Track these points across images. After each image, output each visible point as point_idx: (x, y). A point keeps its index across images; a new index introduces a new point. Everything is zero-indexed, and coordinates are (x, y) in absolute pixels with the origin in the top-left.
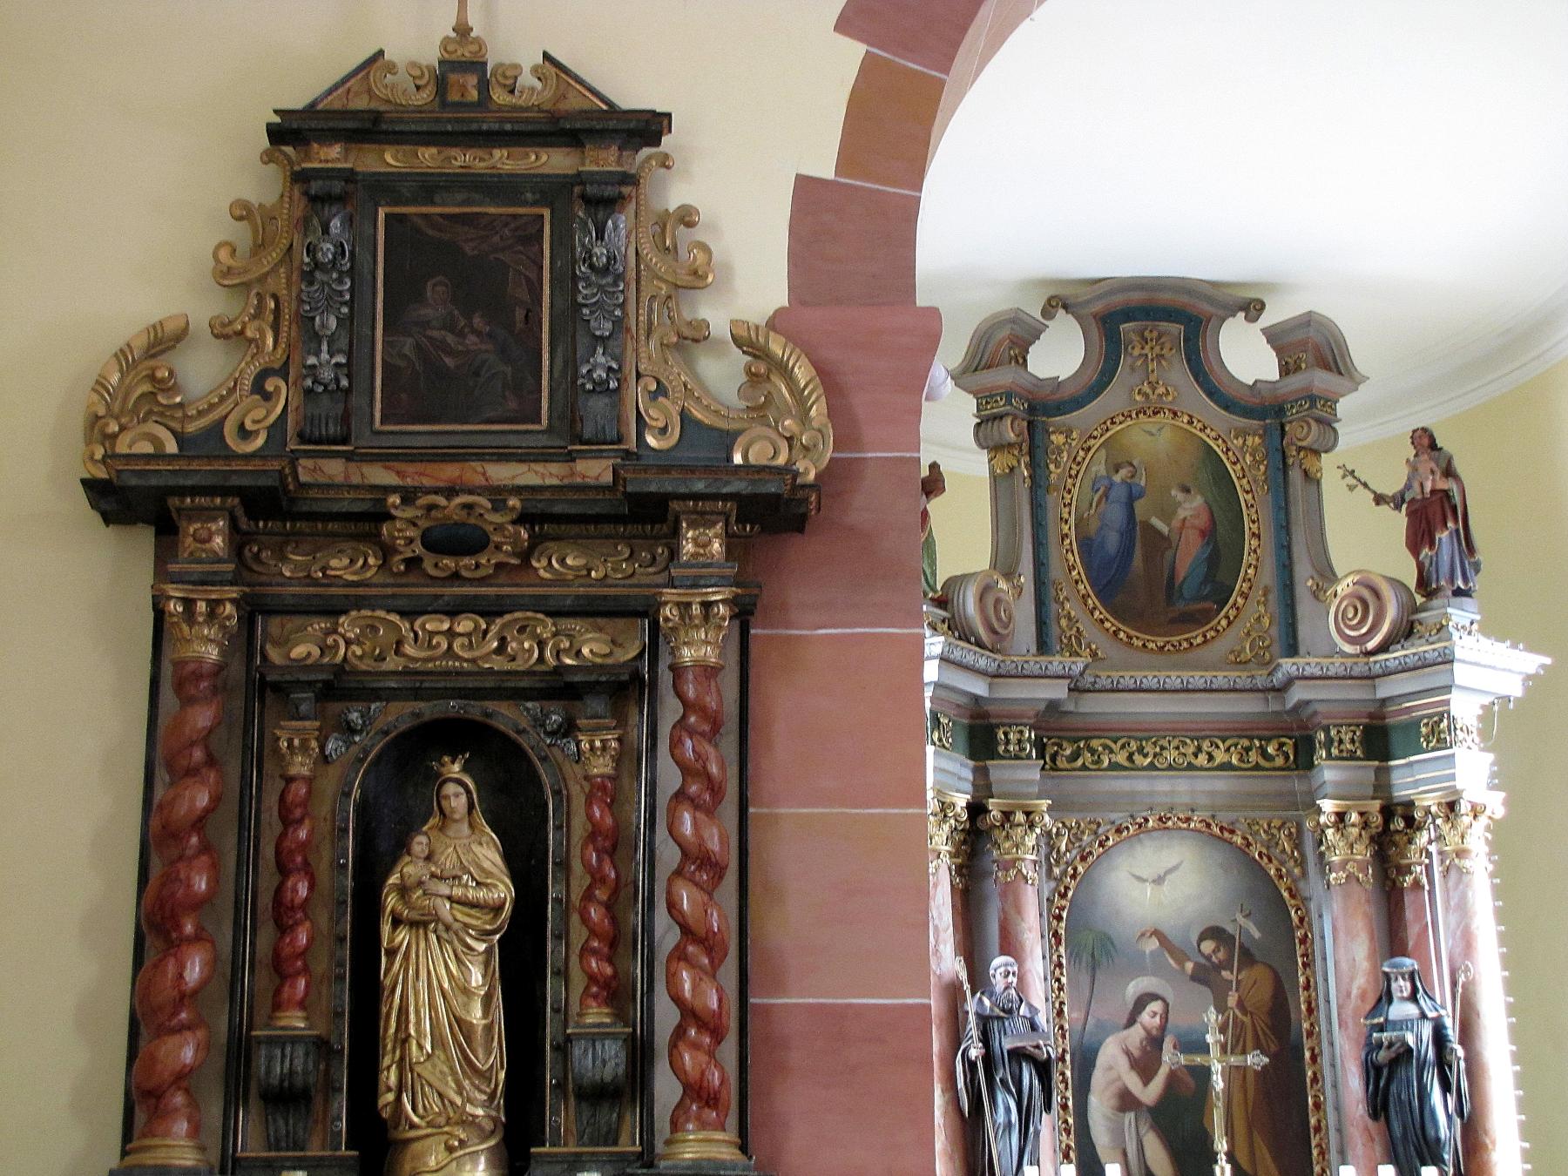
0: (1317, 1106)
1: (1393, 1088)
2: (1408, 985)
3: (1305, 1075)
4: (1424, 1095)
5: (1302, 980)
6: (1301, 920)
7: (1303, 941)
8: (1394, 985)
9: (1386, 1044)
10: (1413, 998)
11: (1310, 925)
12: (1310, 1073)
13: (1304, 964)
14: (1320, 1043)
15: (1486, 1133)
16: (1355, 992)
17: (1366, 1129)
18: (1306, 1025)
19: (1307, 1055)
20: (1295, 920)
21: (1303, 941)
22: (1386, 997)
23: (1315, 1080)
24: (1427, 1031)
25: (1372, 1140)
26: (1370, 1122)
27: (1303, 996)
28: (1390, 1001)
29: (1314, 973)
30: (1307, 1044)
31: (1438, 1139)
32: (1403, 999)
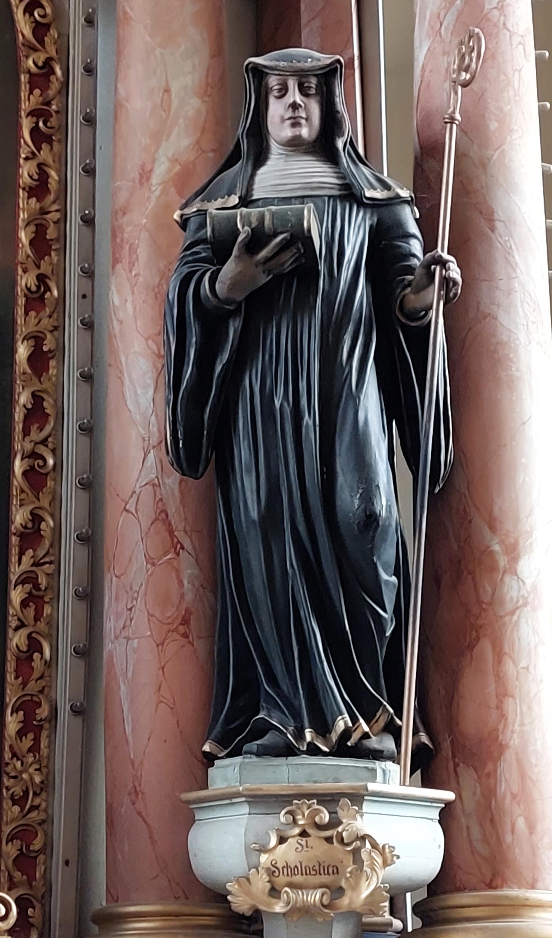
0: (35, 477)
1: (251, 382)
2: (315, 109)
3: (9, 401)
4: (335, 398)
5: (26, 172)
6: (40, 30)
7: (42, 77)
8: (276, 109)
9: (244, 232)
10: (323, 146)
11: (64, 37)
12: (24, 398)
13: (35, 131)
14: (58, 328)
15: (493, 525)
16: (161, 170)
17: (162, 516)
18: (26, 280)
19: (22, 351)
20: (24, 26)
21: (42, 77)
22: (256, 147)
23: (36, 413)
24: (356, 235)
25: (177, 547)
26: (173, 479)
27: (26, 207)
28: (260, 157)
29: (62, 163)
30: (24, 324)
31: (370, 520)
32: (295, 145)
